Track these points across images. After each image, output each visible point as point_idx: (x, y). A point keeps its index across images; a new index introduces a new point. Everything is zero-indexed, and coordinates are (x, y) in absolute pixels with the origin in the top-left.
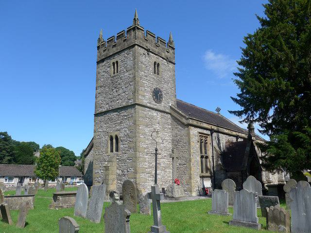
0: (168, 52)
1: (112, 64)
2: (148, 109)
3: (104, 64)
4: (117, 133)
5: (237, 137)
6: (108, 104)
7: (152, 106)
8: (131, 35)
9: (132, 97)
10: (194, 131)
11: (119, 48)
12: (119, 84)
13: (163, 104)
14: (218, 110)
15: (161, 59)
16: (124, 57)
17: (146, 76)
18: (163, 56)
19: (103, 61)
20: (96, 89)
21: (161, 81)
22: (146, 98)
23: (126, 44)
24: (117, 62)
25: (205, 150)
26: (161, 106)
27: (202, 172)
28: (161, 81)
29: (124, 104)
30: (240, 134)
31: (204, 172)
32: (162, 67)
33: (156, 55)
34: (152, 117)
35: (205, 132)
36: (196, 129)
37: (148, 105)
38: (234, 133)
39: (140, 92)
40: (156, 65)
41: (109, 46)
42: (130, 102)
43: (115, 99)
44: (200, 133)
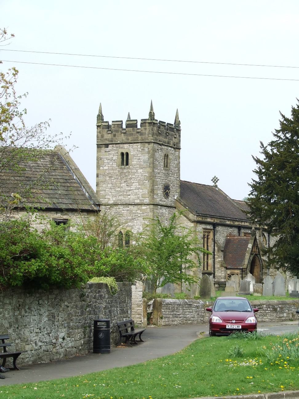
0: (175, 138)
1: (120, 154)
2: (159, 207)
3: (107, 149)
4: (128, 229)
5: (239, 228)
6: (116, 196)
7: (162, 203)
8: (146, 129)
9: (147, 196)
10: (200, 227)
11: (130, 139)
12: (131, 179)
13: (170, 198)
14: (215, 180)
15: (170, 148)
16: (137, 150)
17: (159, 174)
18: (171, 145)
19: (107, 146)
20: (97, 176)
21: (169, 174)
22: (159, 197)
23: (140, 138)
24: (127, 154)
25: (208, 246)
26: (168, 202)
27: (204, 269)
28: (169, 174)
29: (137, 201)
30: (243, 224)
31: (205, 269)
32: (170, 157)
33: (166, 146)
34: (162, 214)
35: (209, 227)
36: (200, 226)
37: (160, 202)
38: (236, 223)
39: (155, 192)
40: (166, 156)
41: (117, 131)
42: (146, 201)
43: (125, 193)
44: (204, 229)
